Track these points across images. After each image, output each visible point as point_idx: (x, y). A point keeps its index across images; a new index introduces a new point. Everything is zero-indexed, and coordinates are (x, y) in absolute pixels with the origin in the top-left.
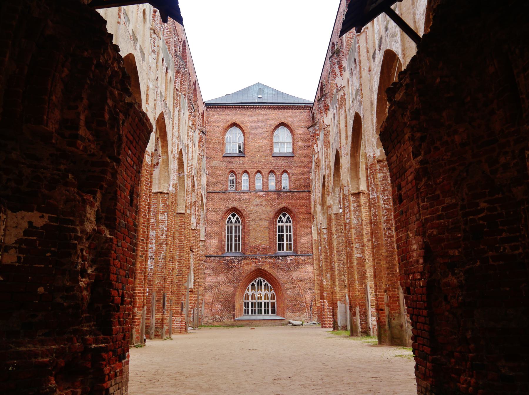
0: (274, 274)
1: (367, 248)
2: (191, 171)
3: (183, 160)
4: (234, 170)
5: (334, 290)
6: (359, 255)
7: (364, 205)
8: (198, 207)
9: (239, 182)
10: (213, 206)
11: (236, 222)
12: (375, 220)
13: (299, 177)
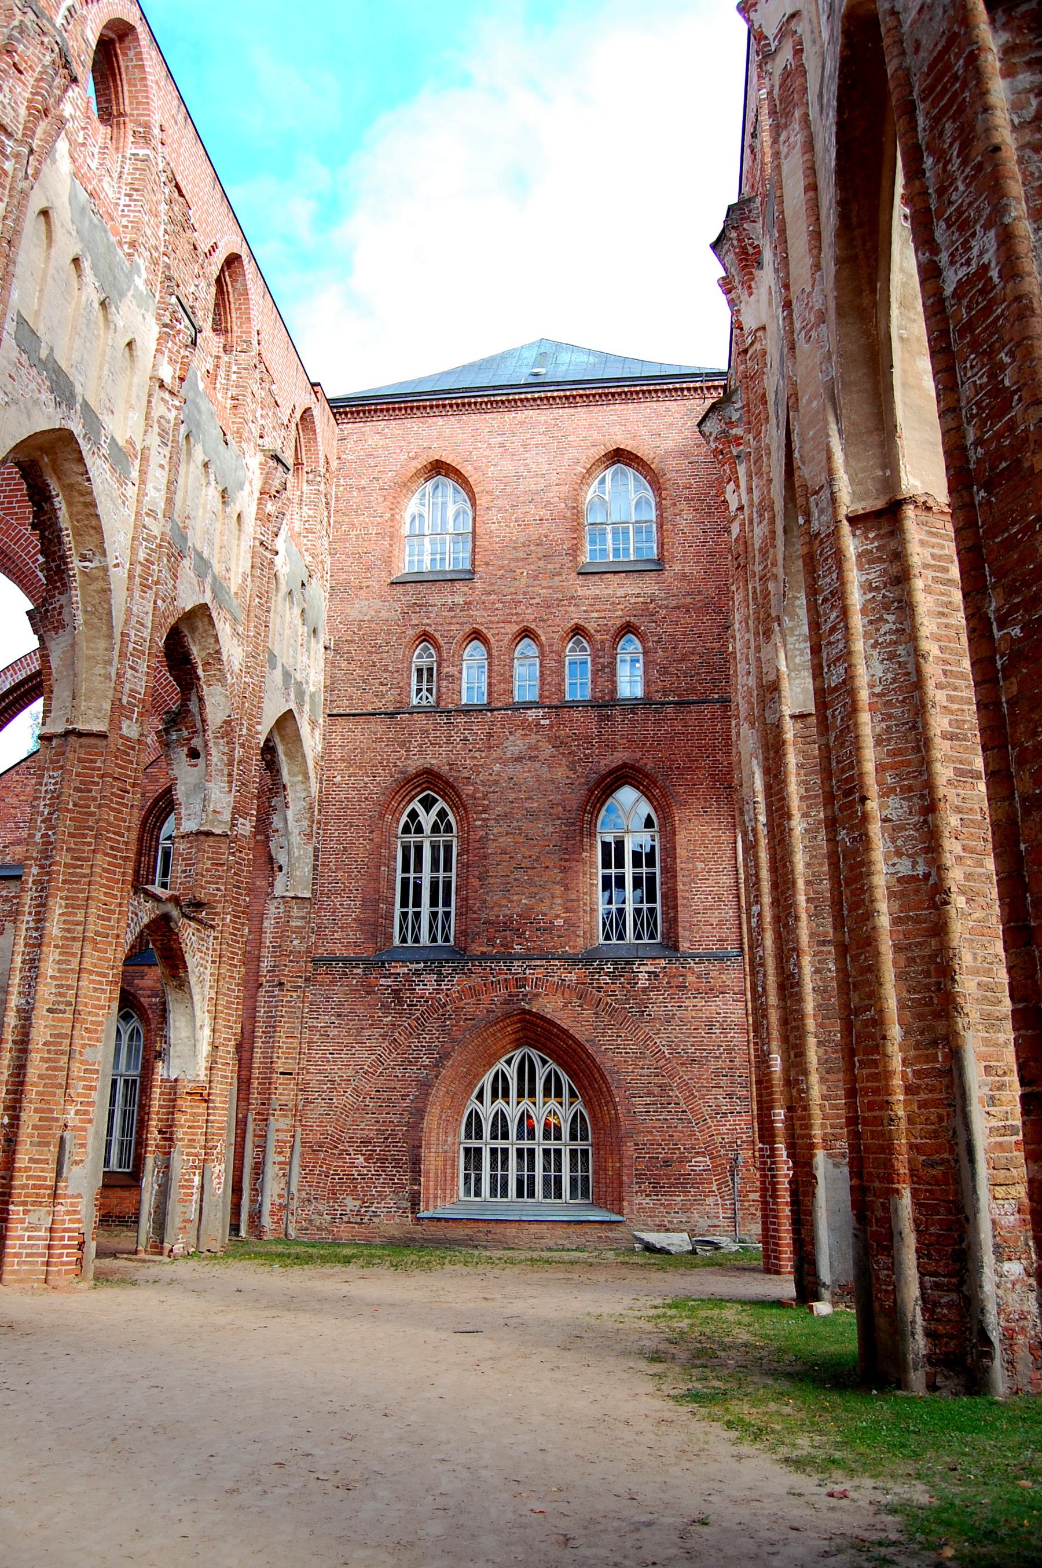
0: (580, 1032)
1: (954, 820)
2: (159, 559)
3: (91, 493)
5: (801, 1091)
6: (904, 867)
7: (929, 574)
8: (242, 745)
9: (448, 675)
10: (348, 768)
11: (435, 829)
12: (998, 436)
13: (682, 648)
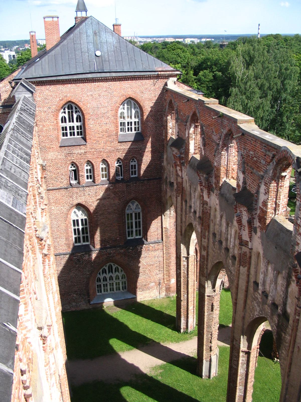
4: (74, 161)
6: (241, 394)
